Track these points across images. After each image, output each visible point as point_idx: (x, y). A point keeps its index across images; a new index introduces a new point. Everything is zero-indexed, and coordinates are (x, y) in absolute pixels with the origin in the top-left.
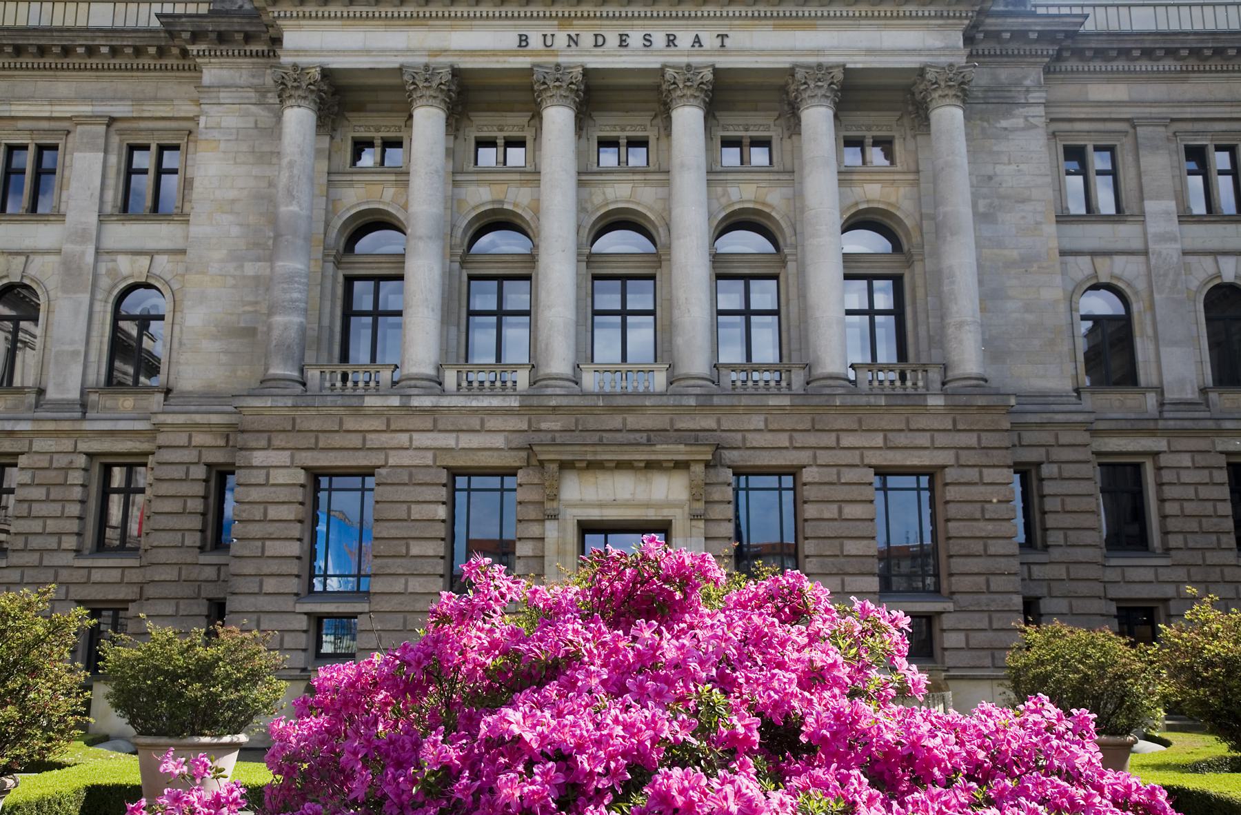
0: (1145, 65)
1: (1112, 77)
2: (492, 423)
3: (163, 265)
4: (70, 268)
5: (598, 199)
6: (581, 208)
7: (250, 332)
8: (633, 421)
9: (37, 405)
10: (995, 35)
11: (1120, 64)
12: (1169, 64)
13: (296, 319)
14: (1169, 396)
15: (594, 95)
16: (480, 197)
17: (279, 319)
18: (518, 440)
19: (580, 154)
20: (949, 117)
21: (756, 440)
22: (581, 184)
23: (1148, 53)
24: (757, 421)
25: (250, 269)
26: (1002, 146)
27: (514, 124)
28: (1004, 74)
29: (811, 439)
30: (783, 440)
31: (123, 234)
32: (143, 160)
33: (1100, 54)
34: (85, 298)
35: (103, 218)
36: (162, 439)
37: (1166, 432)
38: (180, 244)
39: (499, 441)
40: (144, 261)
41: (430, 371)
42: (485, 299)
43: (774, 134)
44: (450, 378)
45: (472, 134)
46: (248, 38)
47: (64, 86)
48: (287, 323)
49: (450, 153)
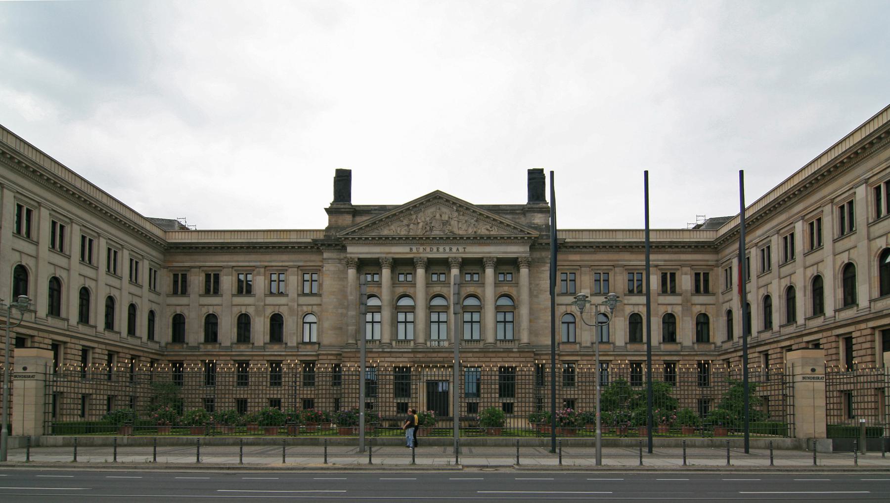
0: (584, 250)
1: (575, 253)
2: (405, 355)
3: (315, 308)
4: (291, 310)
5: (431, 291)
6: (427, 293)
7: (341, 328)
8: (440, 355)
9: (286, 348)
10: (541, 244)
11: (578, 250)
12: (592, 250)
13: (354, 327)
14: (583, 345)
15: (431, 264)
16: (400, 290)
17: (350, 328)
18: (411, 360)
19: (427, 278)
20: (524, 271)
21: (469, 359)
22: (427, 287)
23: (585, 247)
24: (470, 355)
25: (340, 311)
26: (542, 275)
27: (409, 269)
28: (544, 254)
29: (484, 359)
30: (477, 359)
31: (303, 300)
32: (307, 277)
33: (572, 247)
34: (295, 318)
35: (299, 295)
36: (320, 357)
37: (581, 355)
38: (319, 302)
39: (406, 360)
40: (310, 307)
41: (388, 341)
42: (401, 317)
43: (480, 272)
44: (394, 343)
45: (397, 272)
46: (336, 245)
47: (285, 257)
48: (352, 329)
49: (392, 278)
